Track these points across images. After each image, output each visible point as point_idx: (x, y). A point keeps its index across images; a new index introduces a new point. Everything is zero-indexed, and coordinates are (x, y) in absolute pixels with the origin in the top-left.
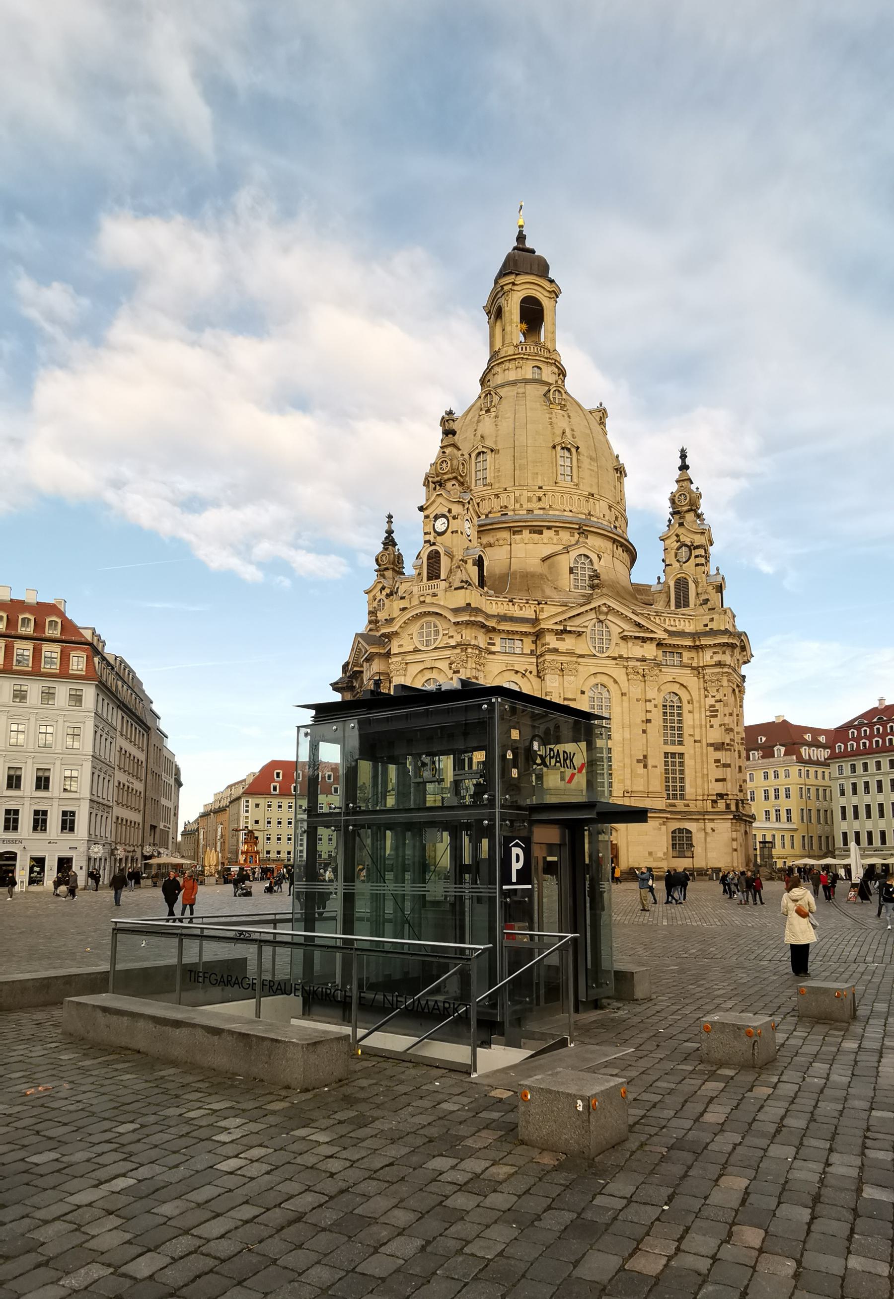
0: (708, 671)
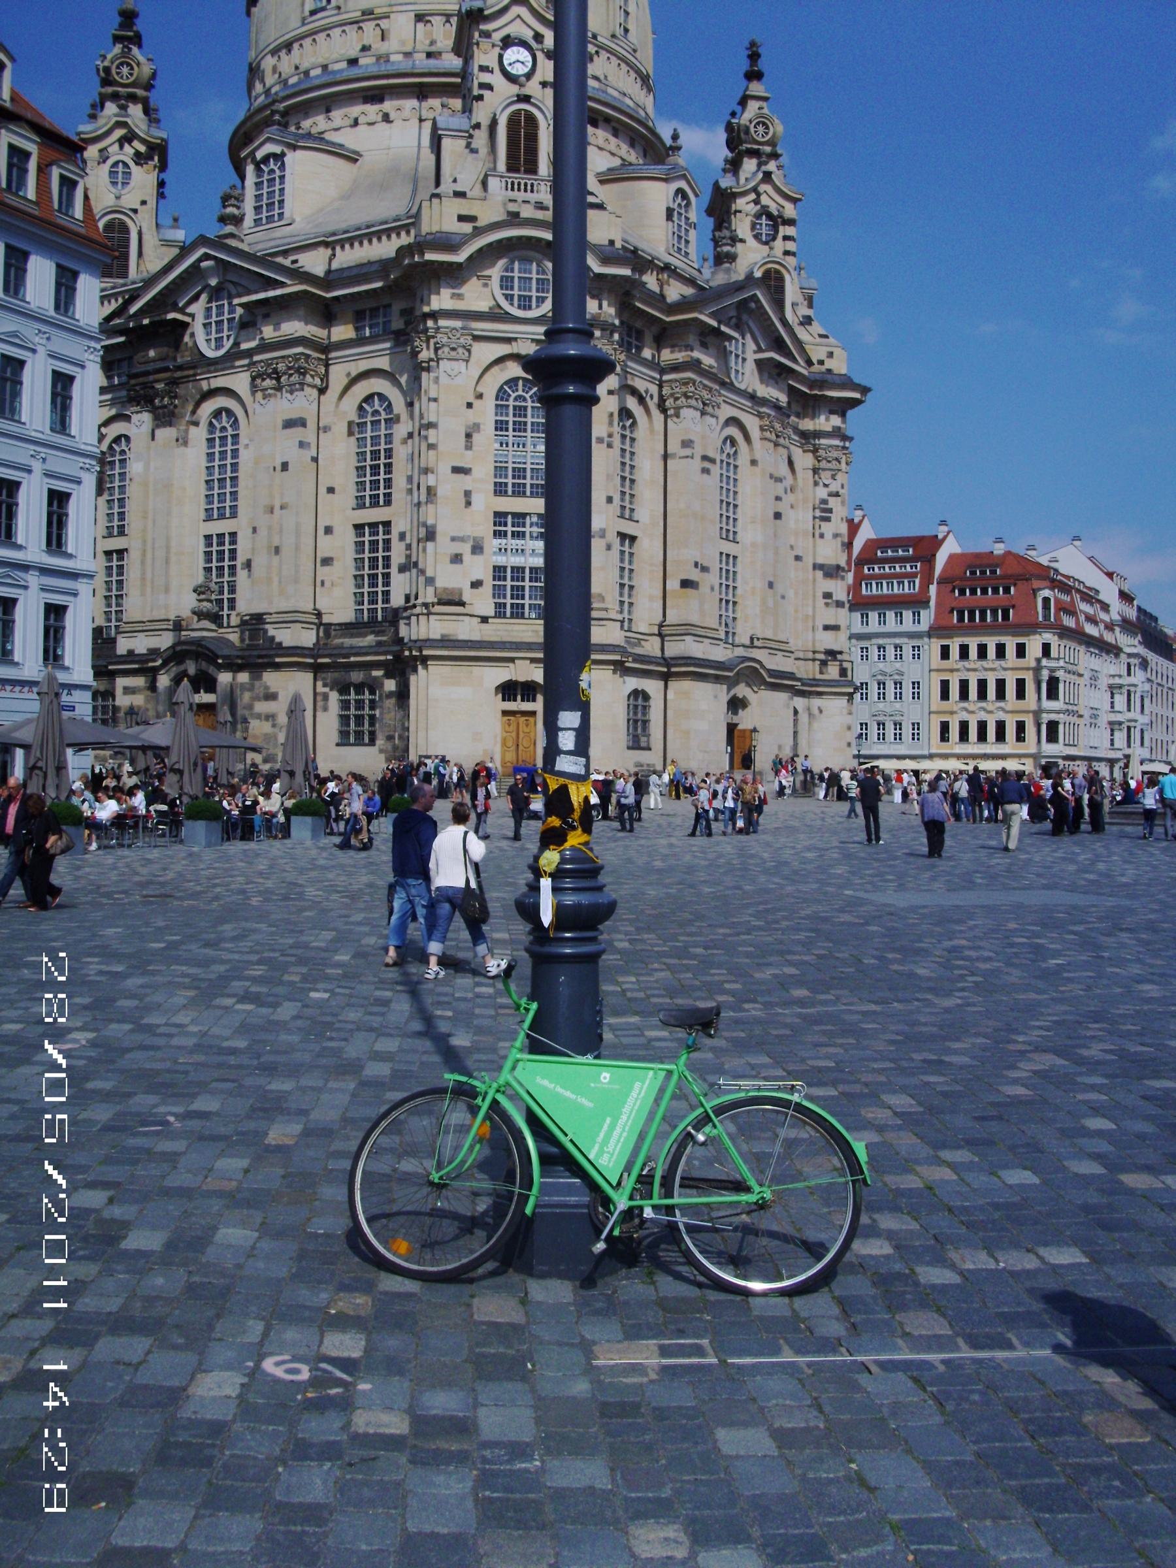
0: (823, 441)
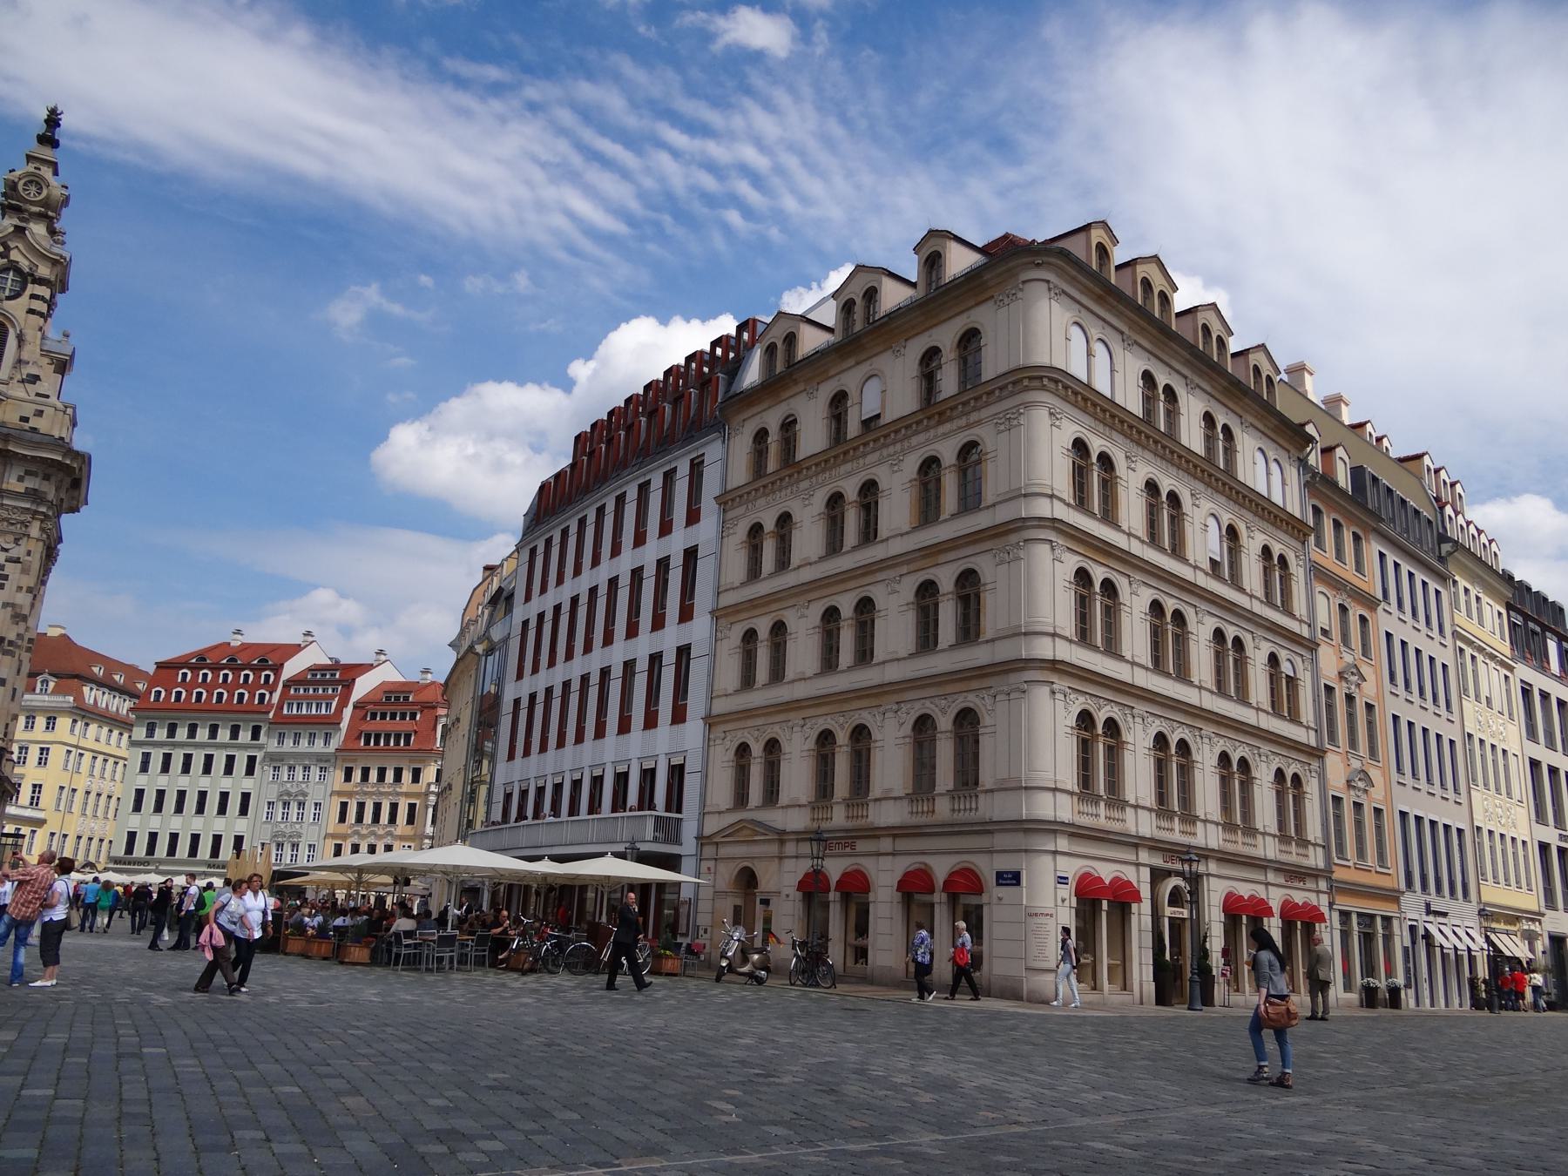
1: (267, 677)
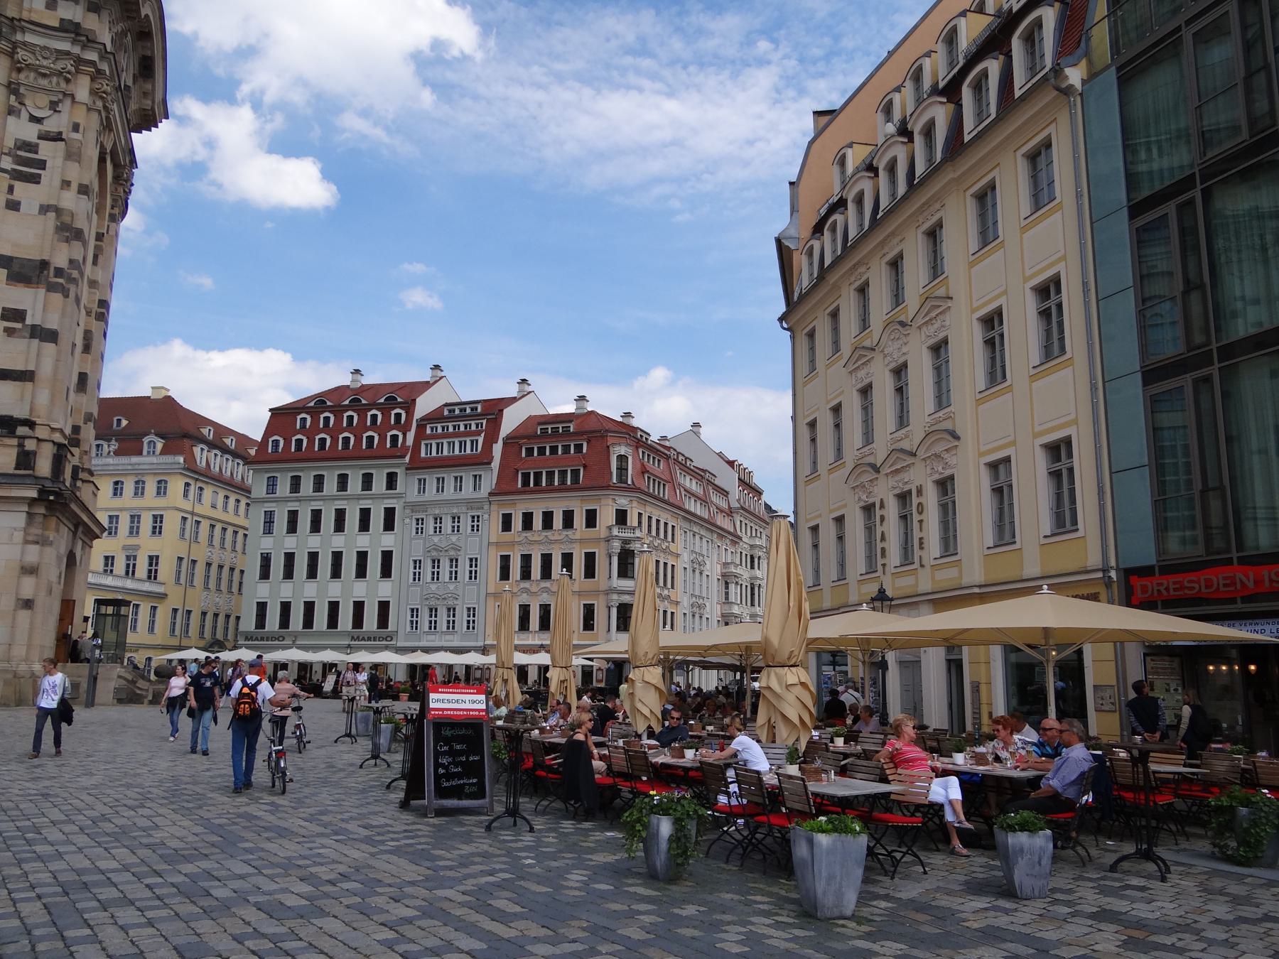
0: (30, 38)
1: (398, 416)
